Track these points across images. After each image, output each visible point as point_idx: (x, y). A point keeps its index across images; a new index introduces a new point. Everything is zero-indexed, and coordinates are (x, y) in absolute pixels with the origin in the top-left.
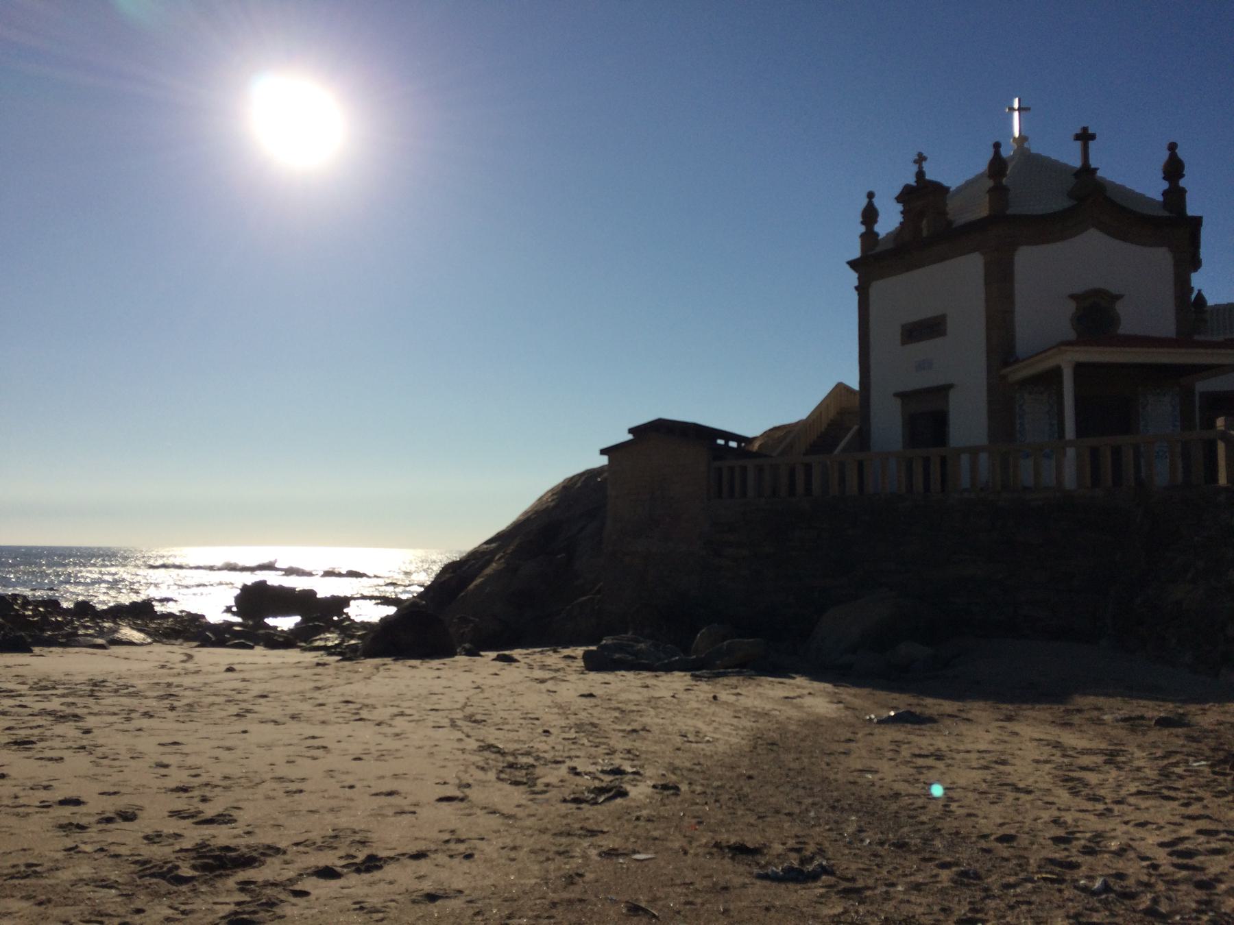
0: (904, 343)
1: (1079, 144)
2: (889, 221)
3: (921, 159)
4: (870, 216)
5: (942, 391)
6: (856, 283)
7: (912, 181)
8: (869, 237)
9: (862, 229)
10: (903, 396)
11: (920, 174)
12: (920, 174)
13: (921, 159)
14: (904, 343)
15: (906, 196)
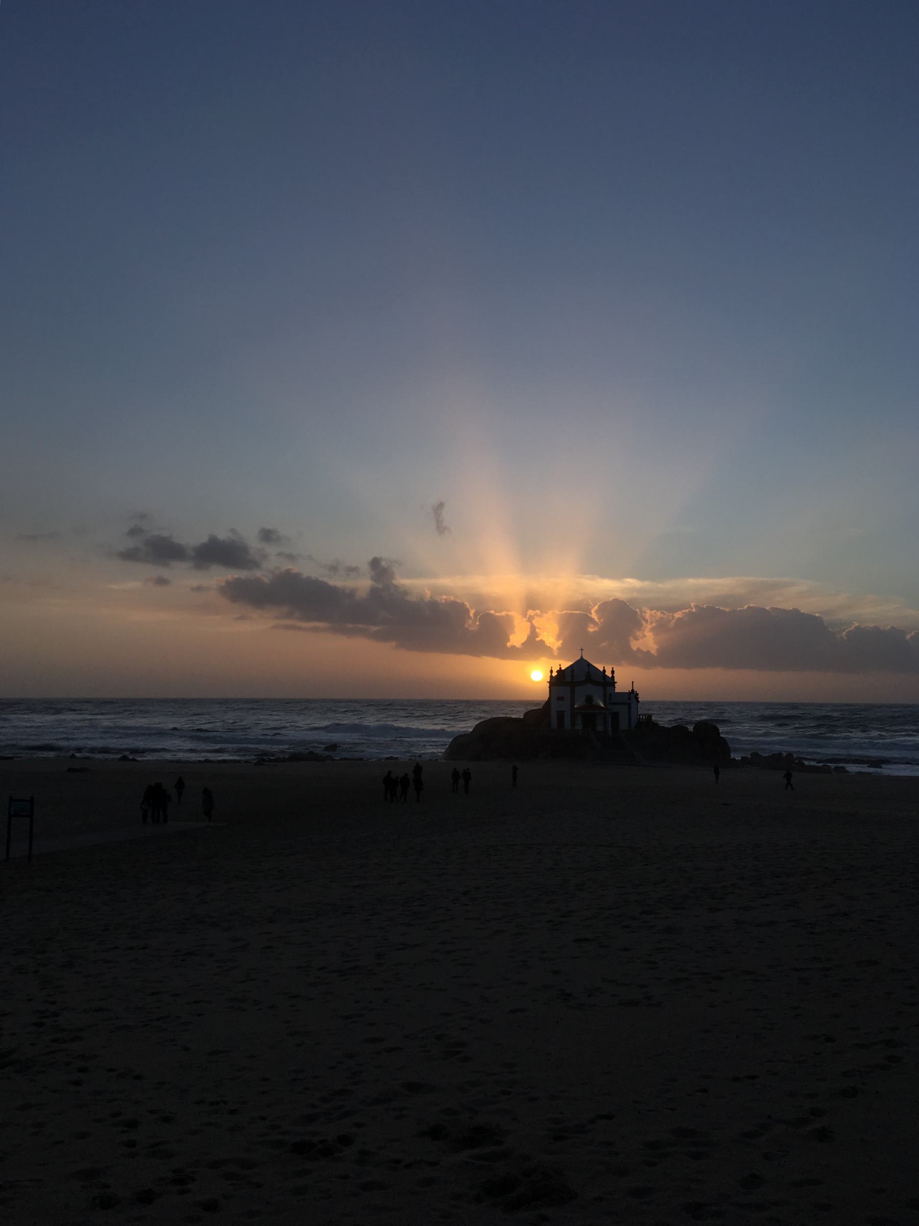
0: (558, 700)
1: (587, 667)
2: (554, 674)
3: (560, 665)
4: (551, 672)
5: (564, 711)
6: (548, 686)
7: (559, 669)
8: (551, 676)
9: (550, 675)
10: (557, 711)
11: (560, 668)
12: (560, 668)
13: (560, 665)
14: (558, 700)
15: (557, 672)
